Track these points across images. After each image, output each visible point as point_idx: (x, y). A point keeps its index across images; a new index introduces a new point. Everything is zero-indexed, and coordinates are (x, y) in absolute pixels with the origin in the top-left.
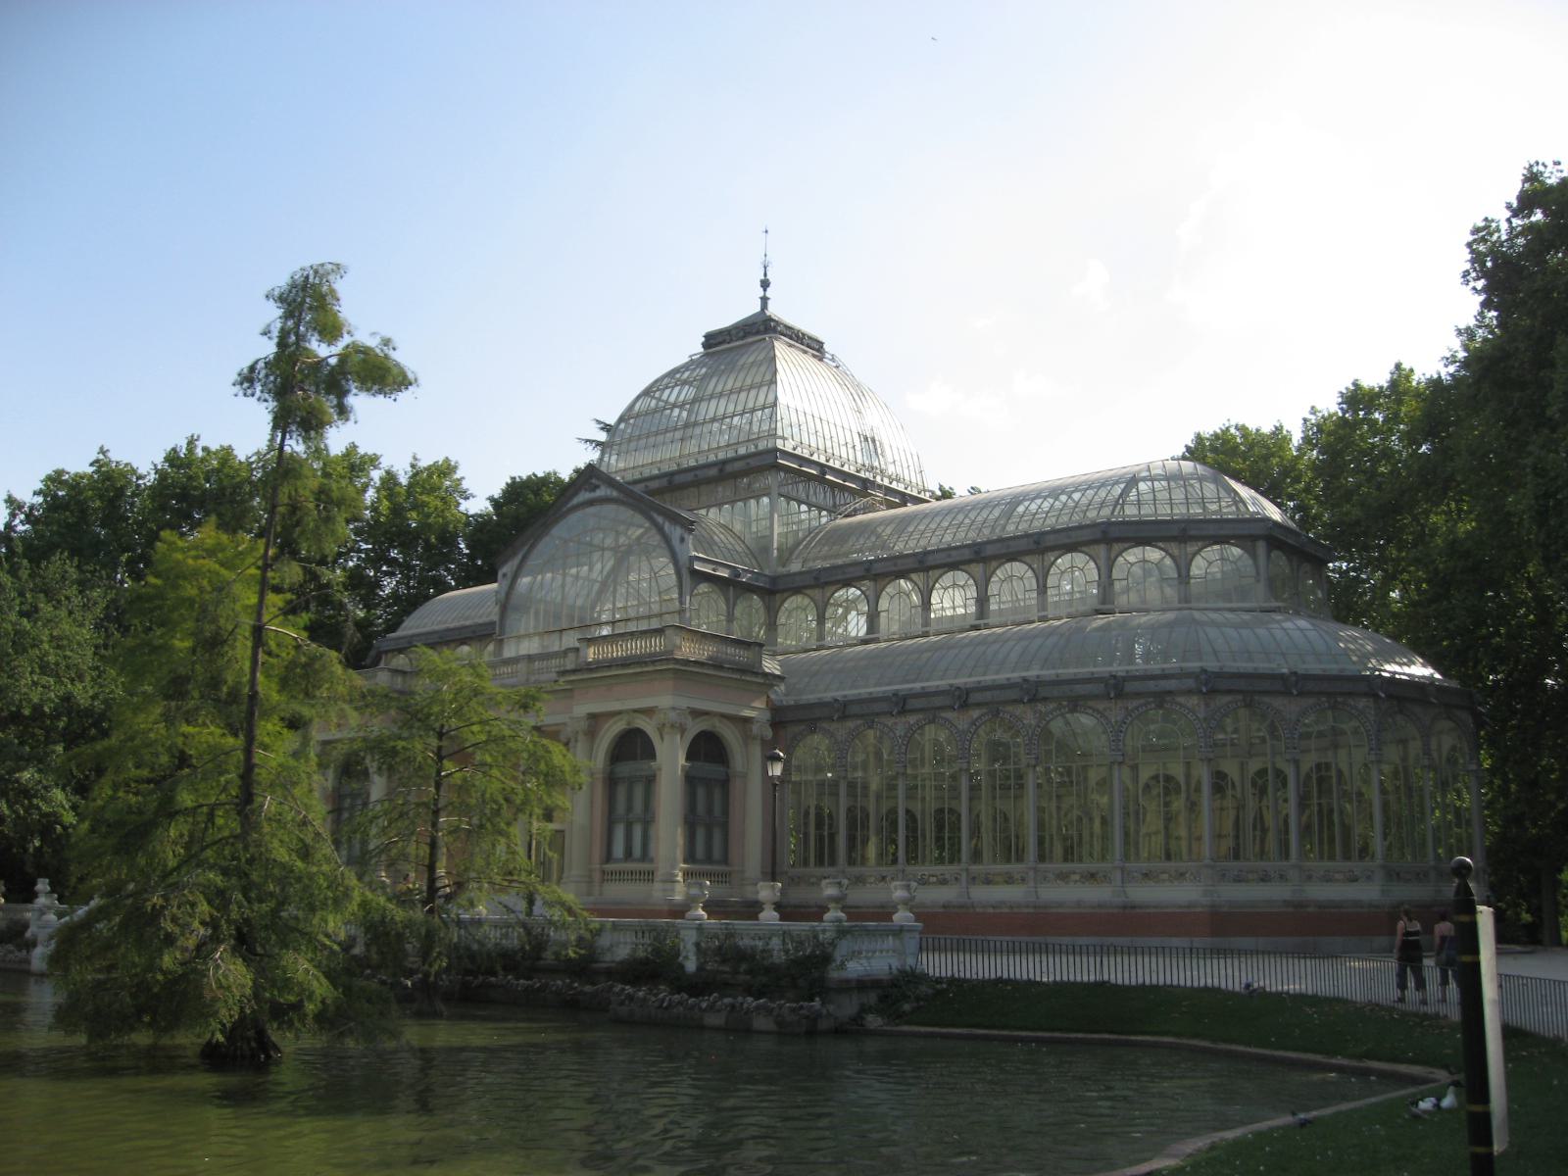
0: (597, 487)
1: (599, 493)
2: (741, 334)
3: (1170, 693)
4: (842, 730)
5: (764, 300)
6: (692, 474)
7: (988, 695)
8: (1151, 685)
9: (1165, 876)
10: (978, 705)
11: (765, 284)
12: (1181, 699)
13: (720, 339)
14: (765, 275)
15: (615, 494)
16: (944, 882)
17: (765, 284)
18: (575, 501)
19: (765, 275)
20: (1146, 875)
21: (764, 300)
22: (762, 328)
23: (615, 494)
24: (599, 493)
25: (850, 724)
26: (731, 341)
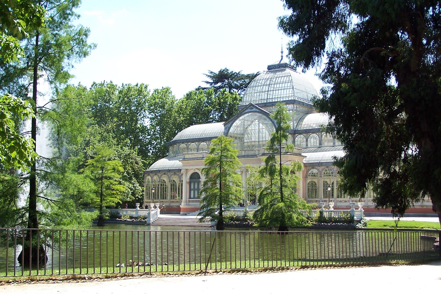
0: (252, 109)
1: (253, 110)
2: (278, 67)
4: (321, 168)
13: (272, 67)
15: (258, 110)
16: (346, 202)
18: (246, 111)
22: (284, 66)
23: (258, 110)
24: (253, 110)
25: (323, 167)
26: (275, 69)
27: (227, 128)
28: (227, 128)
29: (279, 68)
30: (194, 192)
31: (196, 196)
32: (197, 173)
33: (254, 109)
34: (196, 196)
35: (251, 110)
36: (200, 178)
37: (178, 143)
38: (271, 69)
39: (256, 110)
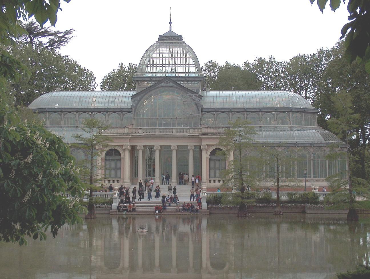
1: (169, 84)
3: (322, 146)
5: (170, 27)
6: (176, 78)
7: (287, 145)
8: (318, 145)
9: (320, 181)
10: (284, 147)
11: (170, 23)
12: (323, 148)
14: (171, 21)
17: (170, 23)
18: (161, 85)
19: (171, 21)
20: (317, 181)
21: (170, 27)
23: (175, 86)
27: (136, 101)
28: (136, 101)
29: (172, 40)
30: (110, 172)
31: (113, 175)
32: (114, 149)
33: (171, 84)
34: (113, 175)
35: (167, 85)
36: (120, 155)
37: (48, 112)
38: (163, 40)
39: (173, 84)
